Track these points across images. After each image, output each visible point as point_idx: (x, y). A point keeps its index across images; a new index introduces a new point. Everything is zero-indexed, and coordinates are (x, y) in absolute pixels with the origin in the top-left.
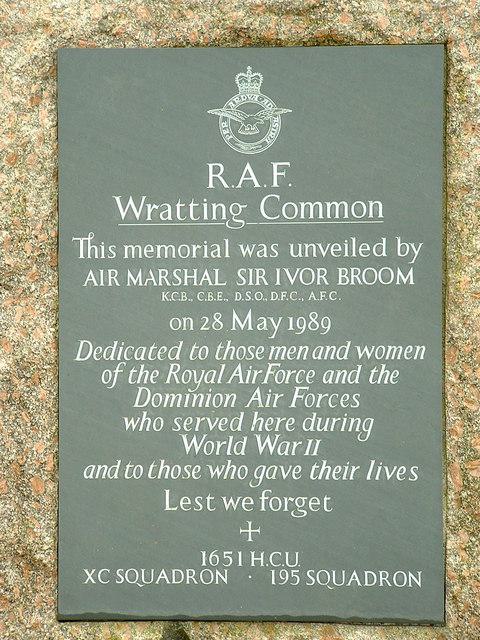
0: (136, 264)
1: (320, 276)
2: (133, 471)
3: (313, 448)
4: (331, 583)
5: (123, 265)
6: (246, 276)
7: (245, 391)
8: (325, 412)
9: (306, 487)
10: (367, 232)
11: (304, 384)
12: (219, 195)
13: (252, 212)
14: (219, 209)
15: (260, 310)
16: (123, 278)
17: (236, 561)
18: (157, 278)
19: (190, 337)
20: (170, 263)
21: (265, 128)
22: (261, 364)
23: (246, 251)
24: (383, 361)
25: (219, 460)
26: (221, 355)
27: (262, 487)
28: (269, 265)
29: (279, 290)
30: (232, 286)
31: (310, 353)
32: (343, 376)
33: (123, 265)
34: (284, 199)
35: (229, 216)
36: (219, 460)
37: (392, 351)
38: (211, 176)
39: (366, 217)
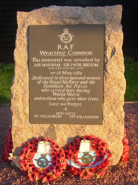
0: (44, 63)
1: (80, 65)
2: (43, 99)
3: (78, 95)
4: (81, 118)
5: (41, 63)
6: (53, 65)
7: (65, 85)
8: (80, 89)
9: (76, 101)
10: (89, 57)
11: (77, 84)
12: (60, 50)
13: (67, 54)
14: (60, 53)
15: (68, 71)
16: (41, 65)
17: (63, 114)
18: (48, 65)
19: (54, 75)
20: (51, 62)
21: (69, 39)
22: (69, 80)
23: (65, 60)
24: (92, 80)
25: (60, 97)
26: (60, 79)
27: (68, 101)
28: (70, 63)
29: (72, 67)
30: (62, 66)
31: (78, 78)
32: (84, 82)
33: (41, 63)
34: (73, 51)
35: (62, 54)
36: (60, 97)
37: (93, 78)
38: (58, 47)
39: (89, 55)
